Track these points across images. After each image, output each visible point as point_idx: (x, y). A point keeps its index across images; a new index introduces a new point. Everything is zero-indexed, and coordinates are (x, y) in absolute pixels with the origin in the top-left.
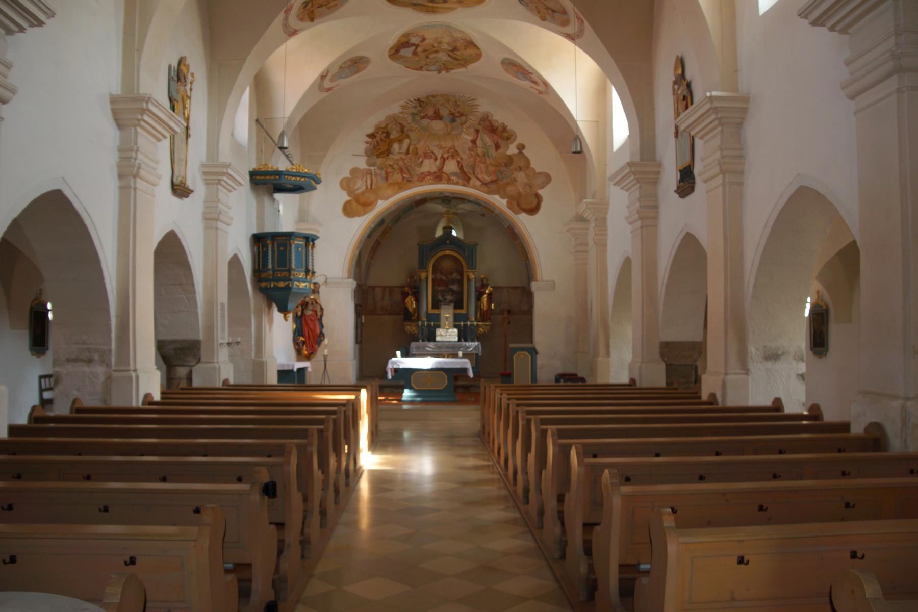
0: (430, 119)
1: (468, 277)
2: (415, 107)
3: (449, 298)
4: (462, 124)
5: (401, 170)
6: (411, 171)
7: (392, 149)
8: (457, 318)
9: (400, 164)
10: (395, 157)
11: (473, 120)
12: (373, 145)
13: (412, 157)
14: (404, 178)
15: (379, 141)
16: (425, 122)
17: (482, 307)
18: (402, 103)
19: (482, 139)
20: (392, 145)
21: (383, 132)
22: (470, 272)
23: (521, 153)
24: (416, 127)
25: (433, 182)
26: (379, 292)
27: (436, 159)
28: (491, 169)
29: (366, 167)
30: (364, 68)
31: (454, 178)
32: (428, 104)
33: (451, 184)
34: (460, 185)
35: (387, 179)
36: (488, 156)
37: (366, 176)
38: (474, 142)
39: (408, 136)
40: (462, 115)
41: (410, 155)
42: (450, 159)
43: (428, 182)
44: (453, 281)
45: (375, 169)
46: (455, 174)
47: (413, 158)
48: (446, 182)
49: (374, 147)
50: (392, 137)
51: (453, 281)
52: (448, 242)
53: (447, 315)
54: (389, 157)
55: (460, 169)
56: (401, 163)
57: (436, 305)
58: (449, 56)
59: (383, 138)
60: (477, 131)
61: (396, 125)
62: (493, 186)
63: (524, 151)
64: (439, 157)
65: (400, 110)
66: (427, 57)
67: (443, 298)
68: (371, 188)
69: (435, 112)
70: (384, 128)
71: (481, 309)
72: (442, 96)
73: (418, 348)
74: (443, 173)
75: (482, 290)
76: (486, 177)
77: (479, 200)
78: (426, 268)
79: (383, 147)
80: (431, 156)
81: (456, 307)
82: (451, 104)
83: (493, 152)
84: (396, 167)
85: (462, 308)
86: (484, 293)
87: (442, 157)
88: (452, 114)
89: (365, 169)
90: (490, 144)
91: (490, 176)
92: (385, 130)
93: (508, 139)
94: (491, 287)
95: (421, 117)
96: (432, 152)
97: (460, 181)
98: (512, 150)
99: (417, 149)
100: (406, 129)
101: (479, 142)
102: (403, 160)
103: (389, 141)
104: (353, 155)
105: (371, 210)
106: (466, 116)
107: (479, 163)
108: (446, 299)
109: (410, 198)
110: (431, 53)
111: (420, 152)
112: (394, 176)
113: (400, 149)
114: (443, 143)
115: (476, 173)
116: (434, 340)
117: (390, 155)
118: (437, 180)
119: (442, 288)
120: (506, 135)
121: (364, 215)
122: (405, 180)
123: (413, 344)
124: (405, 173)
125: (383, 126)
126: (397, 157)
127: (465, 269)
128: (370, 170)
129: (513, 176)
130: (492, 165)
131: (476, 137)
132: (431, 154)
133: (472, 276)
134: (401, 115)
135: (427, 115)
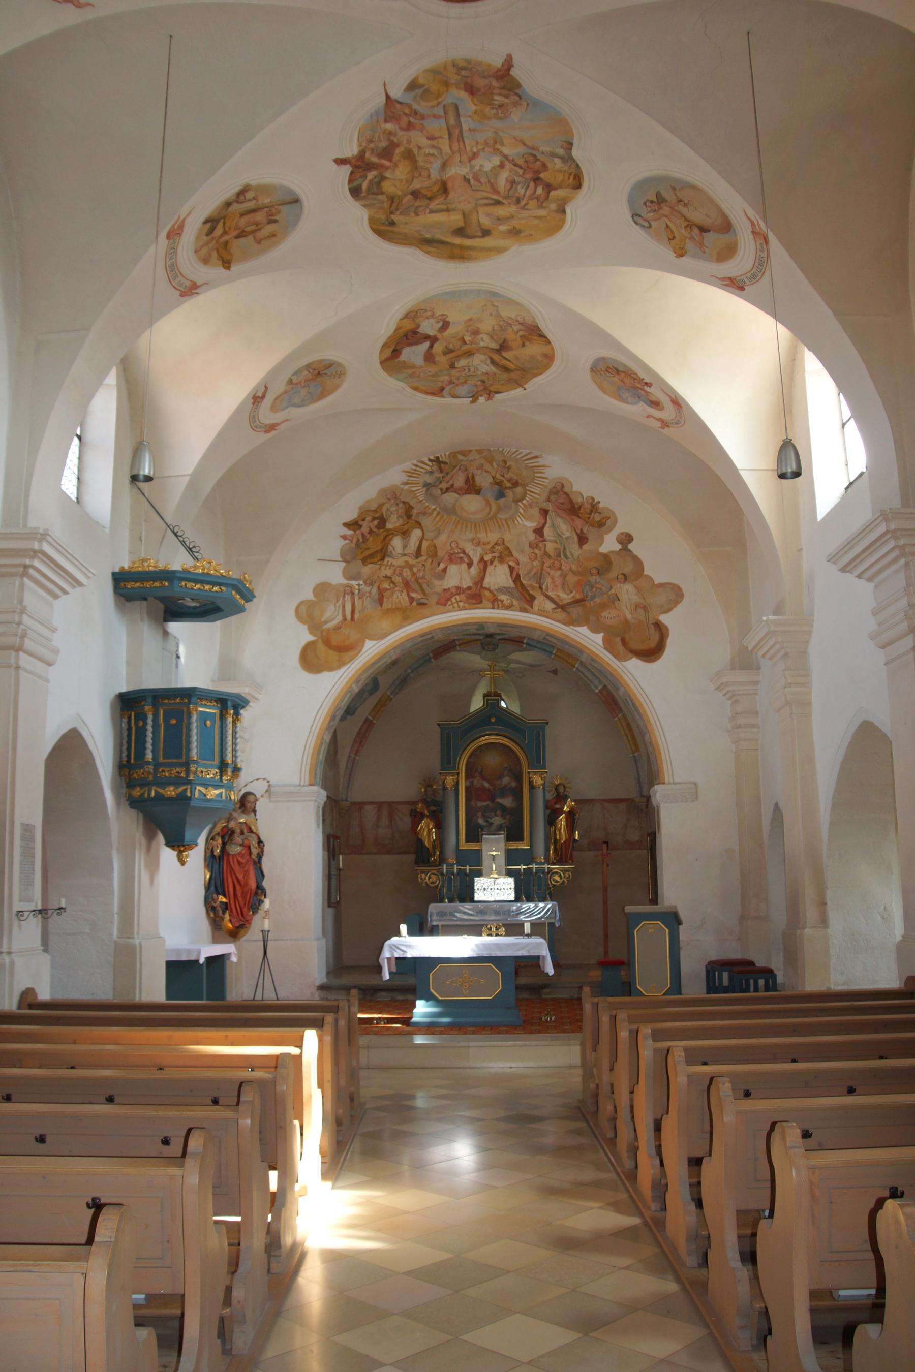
0: (459, 494)
1: (531, 782)
2: (431, 473)
3: (497, 820)
4: (517, 501)
5: (407, 585)
6: (425, 586)
7: (390, 548)
8: (511, 857)
9: (404, 574)
10: (395, 562)
11: (537, 493)
12: (355, 541)
13: (426, 560)
14: (412, 599)
15: (366, 534)
16: (450, 498)
17: (558, 837)
18: (408, 466)
19: (553, 526)
20: (390, 540)
21: (374, 519)
22: (535, 773)
23: (625, 549)
24: (434, 507)
25: (466, 605)
26: (370, 813)
27: (470, 565)
28: (572, 579)
29: (345, 581)
30: (337, 387)
31: (504, 597)
32: (455, 467)
33: (498, 608)
34: (515, 610)
35: (380, 601)
36: (565, 556)
37: (344, 597)
38: (539, 531)
39: (419, 525)
40: (516, 484)
41: (422, 559)
42: (496, 562)
43: (456, 605)
44: (504, 792)
45: (359, 585)
46: (505, 590)
47: (428, 564)
48: (490, 605)
49: (358, 545)
50: (389, 526)
51: (504, 792)
53: (494, 853)
54: (385, 562)
55: (514, 582)
56: (407, 573)
57: (474, 835)
58: (493, 362)
59: (375, 530)
60: (545, 513)
61: (397, 504)
62: (576, 611)
63: (631, 546)
64: (476, 560)
65: (405, 478)
66: (452, 366)
68: (352, 619)
69: (467, 481)
70: (375, 511)
71: (555, 841)
72: (479, 452)
73: (442, 914)
74: (482, 587)
75: (558, 806)
76: (563, 595)
77: (551, 636)
78: (454, 768)
79: (374, 545)
80: (461, 558)
81: (509, 839)
82: (495, 466)
83: (574, 549)
84: (397, 579)
85: (520, 839)
86: (560, 811)
87: (482, 559)
88: (499, 483)
89: (341, 585)
90: (568, 534)
91: (572, 592)
92: (377, 515)
93: (601, 524)
94: (574, 801)
95: (441, 489)
96: (464, 552)
97: (515, 603)
98: (610, 544)
99: (435, 546)
100: (415, 511)
101: (547, 531)
102: (411, 567)
103: (385, 533)
104: (319, 560)
105: (352, 659)
106: (524, 486)
107: (548, 569)
108: (491, 824)
109: (426, 637)
110: (459, 357)
111: (441, 553)
112: (395, 596)
113: (405, 547)
114: (482, 536)
115: (544, 587)
116: (472, 900)
117: (387, 559)
118: (473, 601)
119: (485, 804)
120: (597, 517)
121: (339, 667)
122: (414, 603)
123: (433, 908)
124: (414, 591)
125: (374, 506)
126: (400, 562)
127: (525, 769)
128: (351, 587)
129: (613, 591)
130: (574, 573)
131: (544, 521)
132: (462, 555)
133: (538, 780)
134: (406, 487)
135: (453, 485)
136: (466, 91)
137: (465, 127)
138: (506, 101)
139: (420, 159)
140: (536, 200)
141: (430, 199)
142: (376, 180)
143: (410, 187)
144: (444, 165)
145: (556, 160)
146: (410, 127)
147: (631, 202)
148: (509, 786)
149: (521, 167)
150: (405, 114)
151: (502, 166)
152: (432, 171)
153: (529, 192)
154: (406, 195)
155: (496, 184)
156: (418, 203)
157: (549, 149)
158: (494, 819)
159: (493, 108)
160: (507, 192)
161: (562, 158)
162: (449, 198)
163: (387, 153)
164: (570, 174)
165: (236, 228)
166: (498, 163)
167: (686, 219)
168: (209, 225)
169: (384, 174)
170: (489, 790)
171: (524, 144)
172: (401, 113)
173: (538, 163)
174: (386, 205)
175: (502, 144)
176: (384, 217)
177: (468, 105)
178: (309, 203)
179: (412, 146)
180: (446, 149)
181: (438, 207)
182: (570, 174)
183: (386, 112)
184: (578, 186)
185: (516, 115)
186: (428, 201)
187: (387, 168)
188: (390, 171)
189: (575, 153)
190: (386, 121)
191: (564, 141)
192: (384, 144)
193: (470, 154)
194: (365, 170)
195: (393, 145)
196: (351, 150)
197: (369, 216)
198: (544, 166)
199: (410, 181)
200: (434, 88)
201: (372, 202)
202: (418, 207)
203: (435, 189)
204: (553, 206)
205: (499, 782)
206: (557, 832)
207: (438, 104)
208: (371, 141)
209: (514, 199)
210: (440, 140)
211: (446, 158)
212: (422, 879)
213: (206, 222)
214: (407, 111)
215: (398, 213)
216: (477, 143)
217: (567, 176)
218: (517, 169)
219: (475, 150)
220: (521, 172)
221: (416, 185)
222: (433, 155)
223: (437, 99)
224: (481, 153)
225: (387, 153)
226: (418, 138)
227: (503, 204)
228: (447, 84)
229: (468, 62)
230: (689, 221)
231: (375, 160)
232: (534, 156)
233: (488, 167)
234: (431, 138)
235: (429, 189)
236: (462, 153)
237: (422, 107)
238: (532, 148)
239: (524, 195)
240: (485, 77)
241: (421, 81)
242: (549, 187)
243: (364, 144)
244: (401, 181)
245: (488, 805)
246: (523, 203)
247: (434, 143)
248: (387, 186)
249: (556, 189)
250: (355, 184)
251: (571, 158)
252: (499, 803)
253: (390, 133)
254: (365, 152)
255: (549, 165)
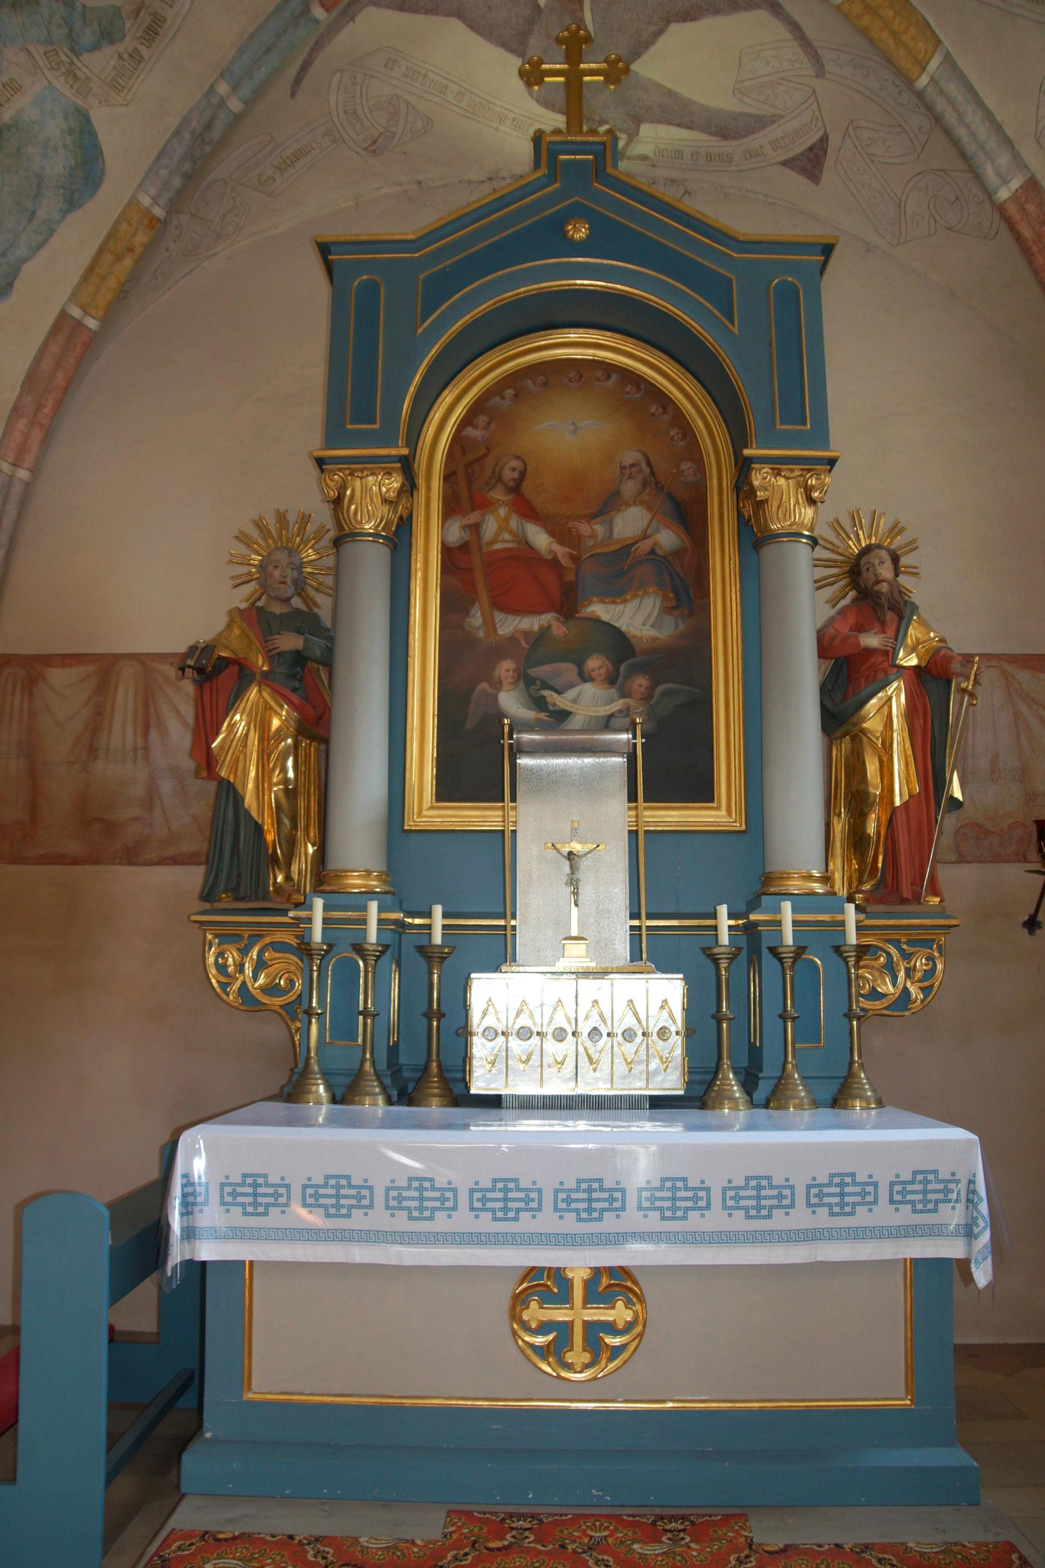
52: (580, 232)
67: (540, 704)
75: (872, 640)
108: (562, 716)
119: (532, 623)
148: (645, 546)
158: (571, 693)
170: (555, 562)
205: (600, 529)
206: (872, 768)
212: (222, 968)
245: (545, 630)
252: (598, 621)
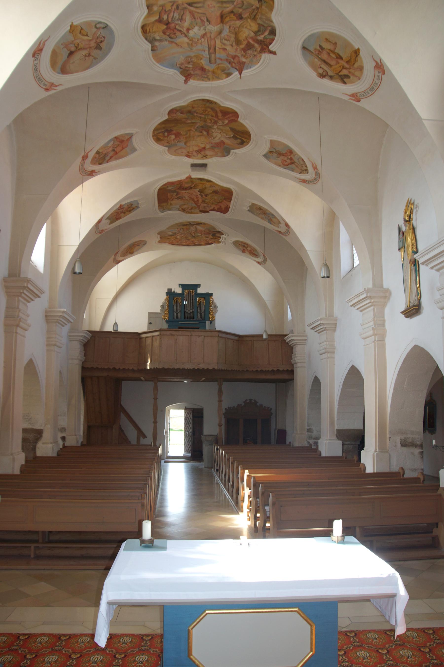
136: (205, 69)
137: (207, 53)
138: (186, 65)
139: (233, 39)
140: (167, 10)
141: (232, 12)
142: (259, 33)
143: (242, 22)
144: (220, 33)
145: (158, 38)
146: (234, 57)
147: (111, 33)
149: (178, 30)
150: (235, 64)
151: (188, 30)
152: (228, 31)
153: (171, 15)
154: (246, 18)
155: (191, 18)
156: (240, 10)
157: (163, 43)
159: (193, 61)
160: (185, 12)
161: (156, 40)
162: (220, 11)
163: (249, 46)
164: (149, 32)
165: (338, 63)
166: (190, 32)
167: (81, 49)
168: (345, 80)
169: (254, 35)
171: (176, 44)
172: (236, 64)
173: (168, 34)
174: (259, 16)
175: (188, 43)
176: (263, 7)
177: (204, 63)
178: (299, 43)
179: (235, 47)
180: (218, 42)
181: (228, 5)
182: (149, 32)
183: (244, 67)
184: (143, 27)
185: (181, 59)
186: (234, 11)
187: (252, 38)
188: (250, 36)
189: (149, 46)
190: (245, 63)
191: (156, 50)
192: (249, 52)
193: (205, 37)
194: (263, 42)
195: (244, 50)
196: (265, 56)
197: (271, 13)
198: (164, 33)
199: (241, 26)
200: (219, 72)
201: (266, 22)
202: (240, 8)
203: (228, 19)
204: (155, 8)
207: (218, 65)
208: (255, 55)
209: (180, 8)
210: (220, 47)
211: (219, 37)
213: (345, 83)
214: (234, 65)
215: (254, 7)
216: (201, 44)
217: (151, 31)
218: (180, 29)
219: (203, 40)
220: (177, 27)
221: (238, 23)
222: (225, 40)
223: (219, 67)
224: (199, 38)
225: (249, 46)
226: (231, 50)
227: (187, 4)
228: (213, 72)
229: (203, 80)
230: (79, 49)
231: (256, 45)
232: (170, 38)
233: (196, 29)
234: (224, 49)
235: (231, 19)
236: (210, 38)
237: (227, 65)
238: (172, 42)
239: (174, 12)
240: (196, 74)
241: (224, 76)
242: (160, 21)
243: (258, 55)
244: (246, 28)
246: (174, 7)
247: (223, 47)
248: (255, 27)
249: (156, 21)
250: (271, 37)
251: (150, 42)
253: (244, 56)
254: (260, 51)
255: (162, 34)
